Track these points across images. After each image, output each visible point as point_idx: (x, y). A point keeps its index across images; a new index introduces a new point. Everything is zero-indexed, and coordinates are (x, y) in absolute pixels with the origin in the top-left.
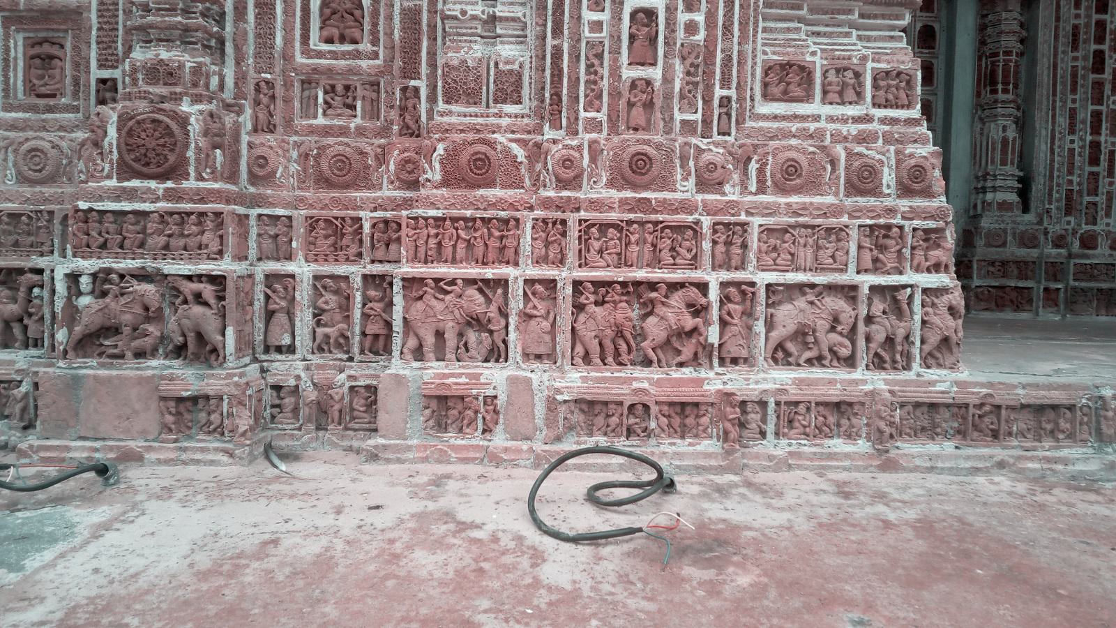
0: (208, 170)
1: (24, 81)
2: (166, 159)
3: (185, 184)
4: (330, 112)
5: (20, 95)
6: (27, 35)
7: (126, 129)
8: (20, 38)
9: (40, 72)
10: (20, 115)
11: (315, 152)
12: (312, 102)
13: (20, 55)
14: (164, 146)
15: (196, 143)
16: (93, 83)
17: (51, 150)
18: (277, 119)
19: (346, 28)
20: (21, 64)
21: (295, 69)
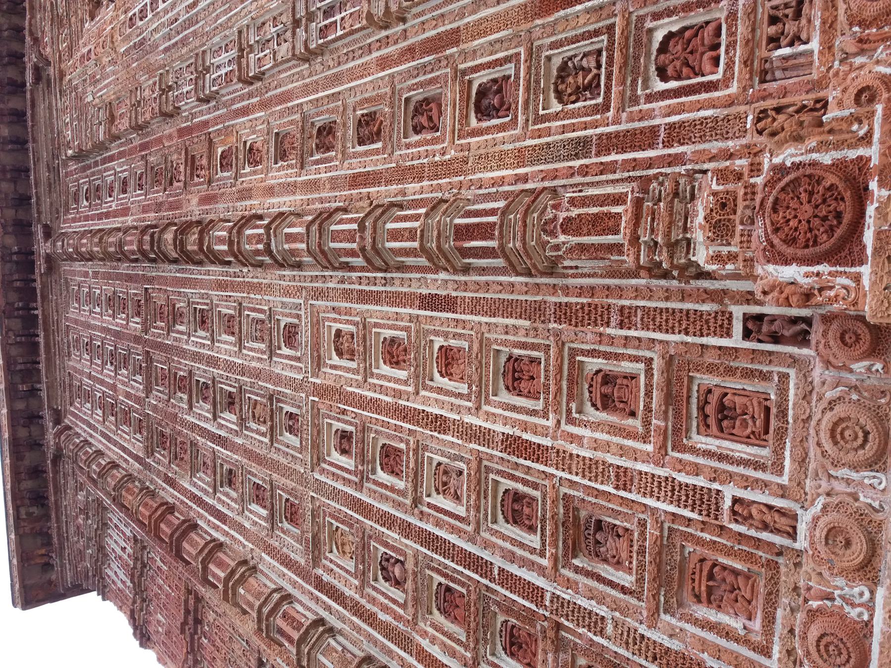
0: (855, 127)
1: (748, 444)
2: (832, 187)
3: (875, 161)
4: (804, 36)
5: (765, 452)
6: (694, 429)
7: (783, 248)
8: (696, 438)
9: (738, 423)
10: (787, 454)
11: (856, 29)
12: (791, 63)
13: (718, 442)
14: (811, 194)
15: (812, 151)
16: (748, 345)
17: (835, 412)
18: (807, 99)
19: (703, 44)
20: (726, 444)
21: (745, 89)
